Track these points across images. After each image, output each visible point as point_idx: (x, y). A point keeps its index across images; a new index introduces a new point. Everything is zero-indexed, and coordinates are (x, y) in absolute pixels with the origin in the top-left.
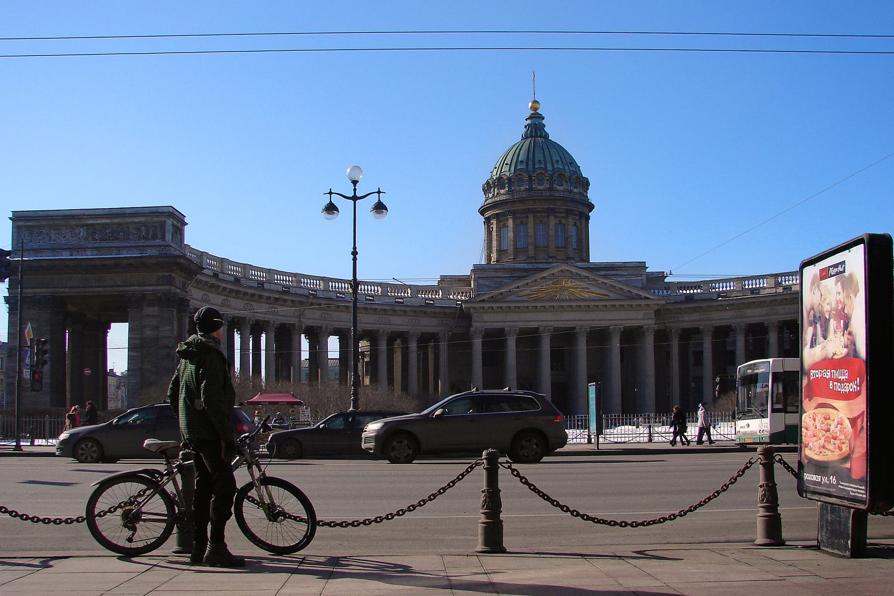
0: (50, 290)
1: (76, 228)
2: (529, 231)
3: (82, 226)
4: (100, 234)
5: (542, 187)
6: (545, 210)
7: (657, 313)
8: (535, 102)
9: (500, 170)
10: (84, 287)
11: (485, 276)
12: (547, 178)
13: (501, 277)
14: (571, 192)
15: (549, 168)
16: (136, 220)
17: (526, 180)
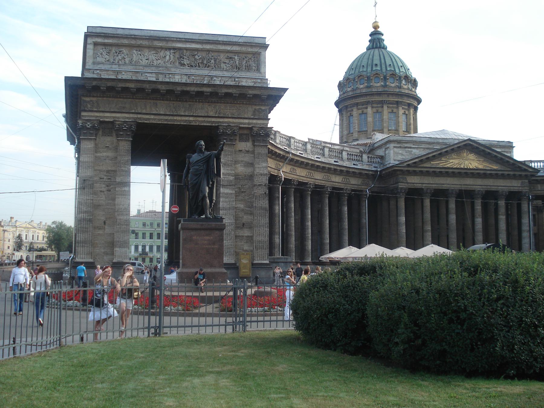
0: (132, 116)
1: (161, 51)
2: (384, 117)
3: (170, 49)
4: (189, 60)
5: (393, 85)
6: (395, 102)
7: (530, 182)
9: (357, 70)
10: (172, 115)
12: (397, 78)
13: (411, 148)
14: (411, 90)
15: (397, 71)
16: (229, 48)
17: (382, 79)
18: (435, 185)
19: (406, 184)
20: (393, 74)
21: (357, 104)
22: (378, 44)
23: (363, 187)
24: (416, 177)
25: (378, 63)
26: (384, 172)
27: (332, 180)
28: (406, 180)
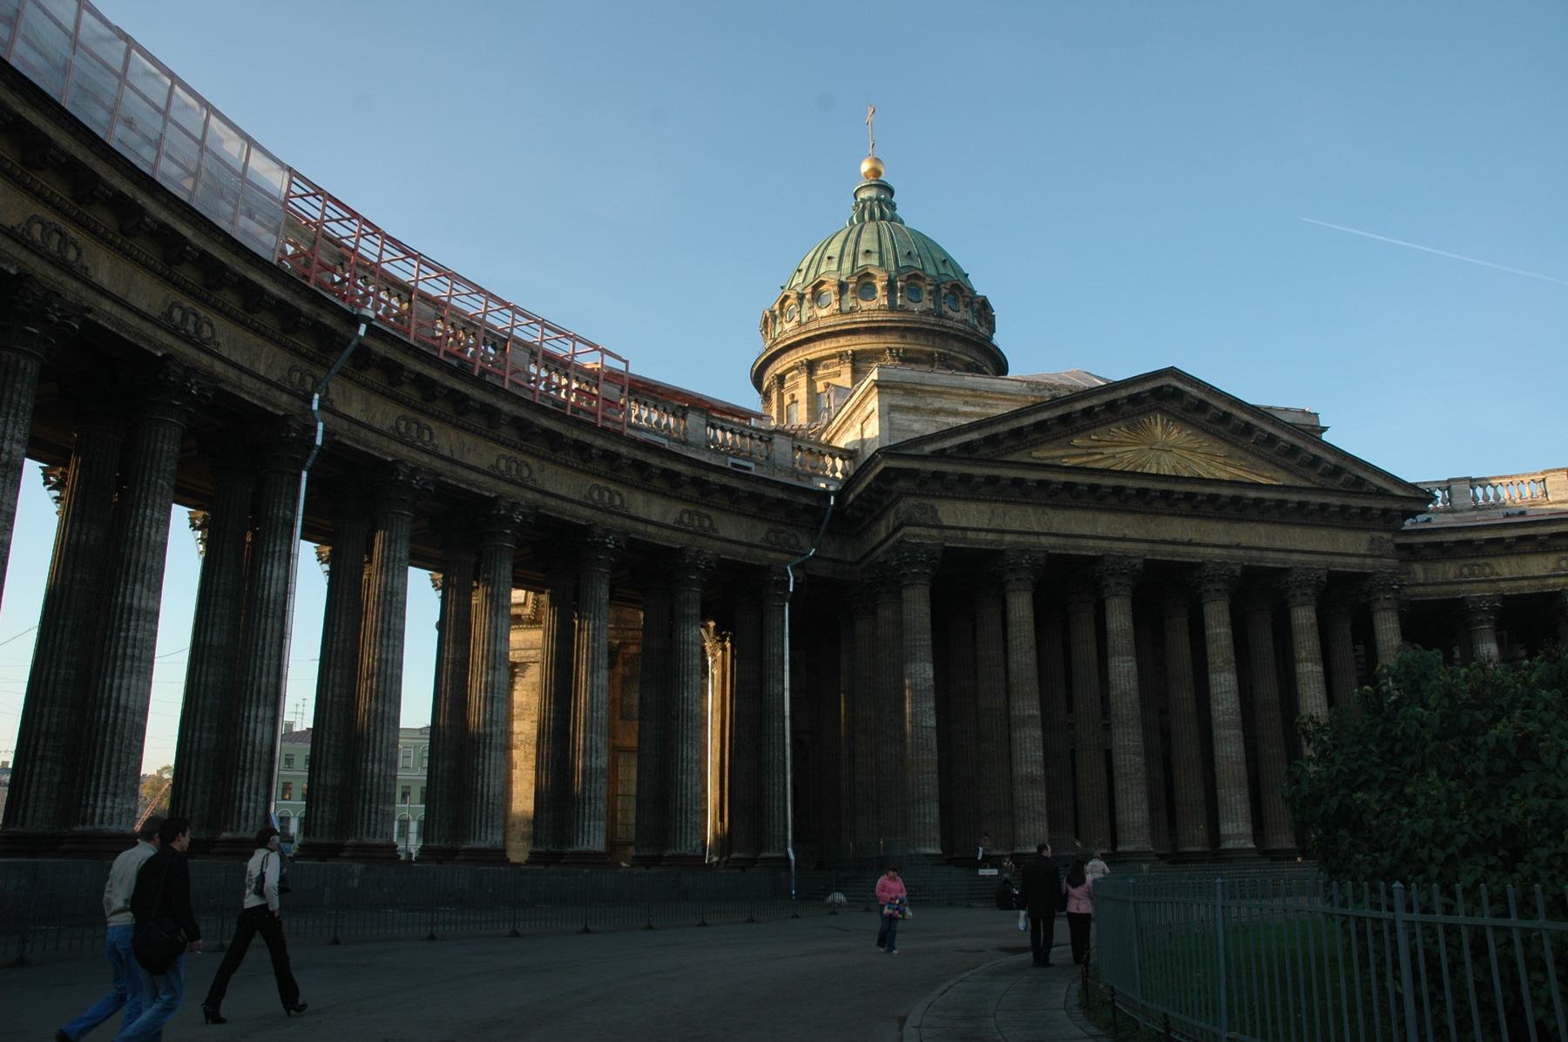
5: (916, 308)
6: (924, 357)
8: (877, 160)
9: (812, 271)
11: (912, 404)
12: (929, 288)
13: (956, 414)
15: (931, 270)
18: (1052, 540)
19: (935, 532)
20: (916, 276)
21: (811, 366)
22: (877, 211)
23: (772, 555)
24: (973, 506)
25: (875, 247)
26: (851, 497)
27: (632, 512)
28: (935, 516)
